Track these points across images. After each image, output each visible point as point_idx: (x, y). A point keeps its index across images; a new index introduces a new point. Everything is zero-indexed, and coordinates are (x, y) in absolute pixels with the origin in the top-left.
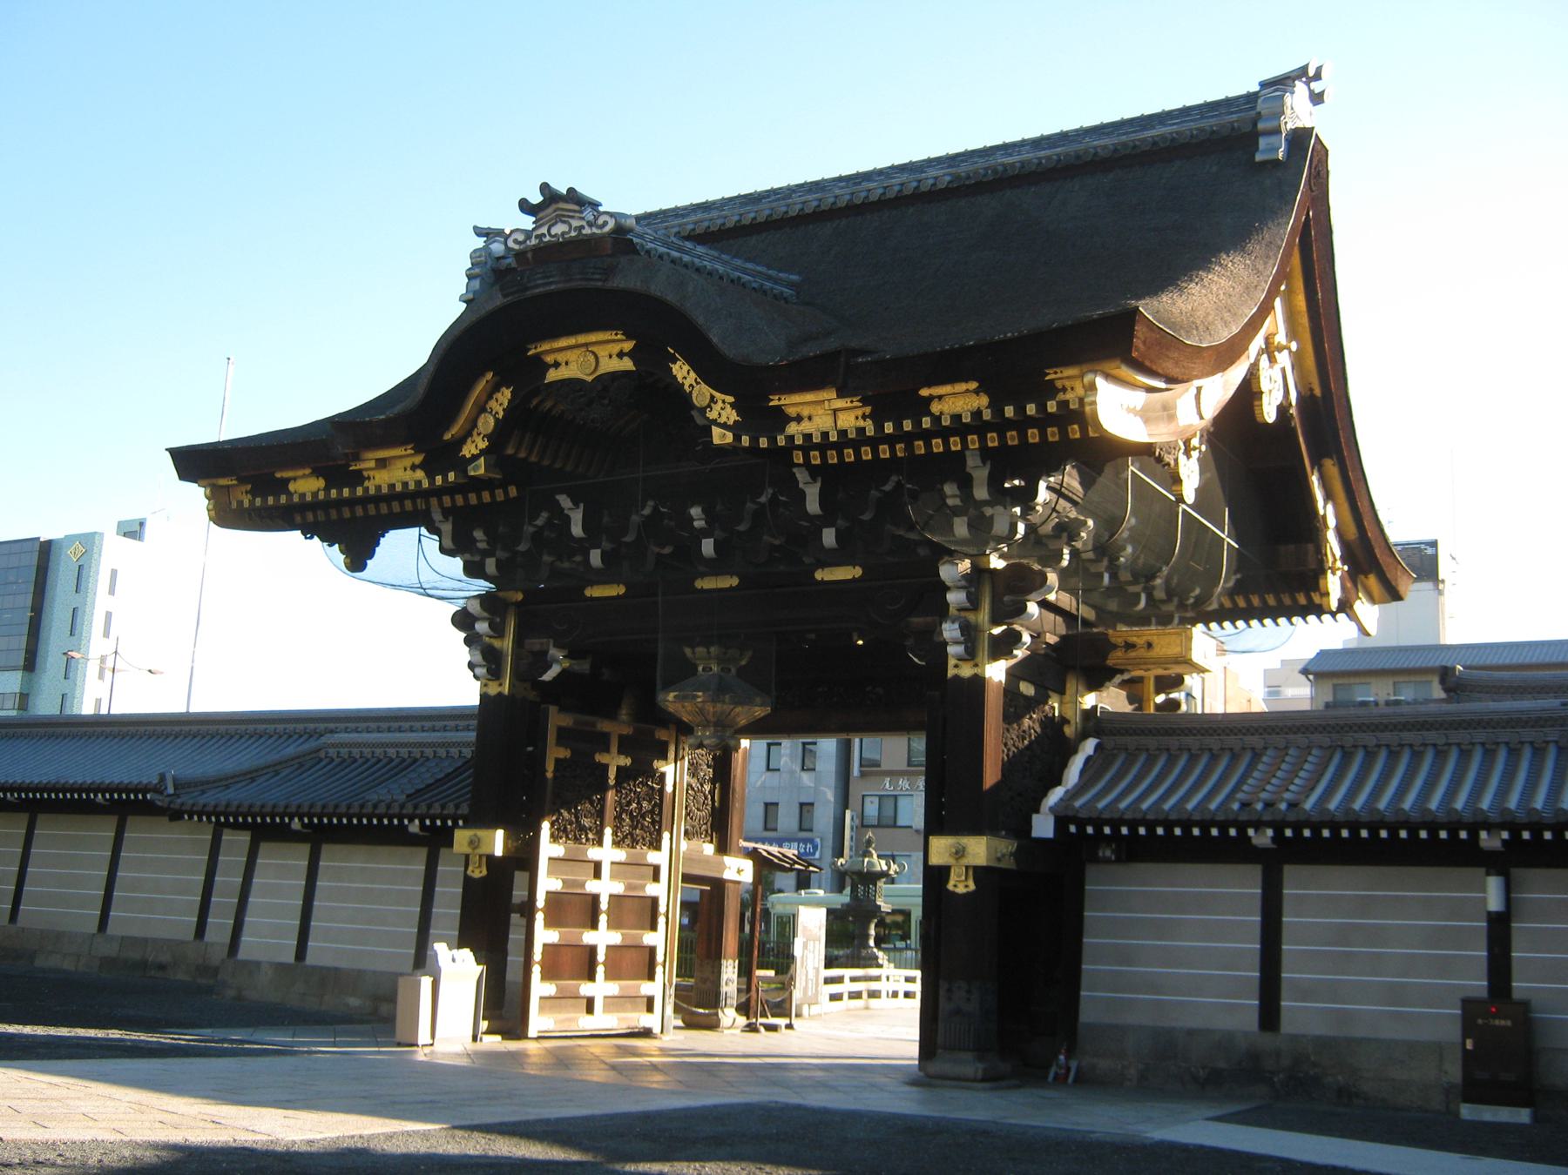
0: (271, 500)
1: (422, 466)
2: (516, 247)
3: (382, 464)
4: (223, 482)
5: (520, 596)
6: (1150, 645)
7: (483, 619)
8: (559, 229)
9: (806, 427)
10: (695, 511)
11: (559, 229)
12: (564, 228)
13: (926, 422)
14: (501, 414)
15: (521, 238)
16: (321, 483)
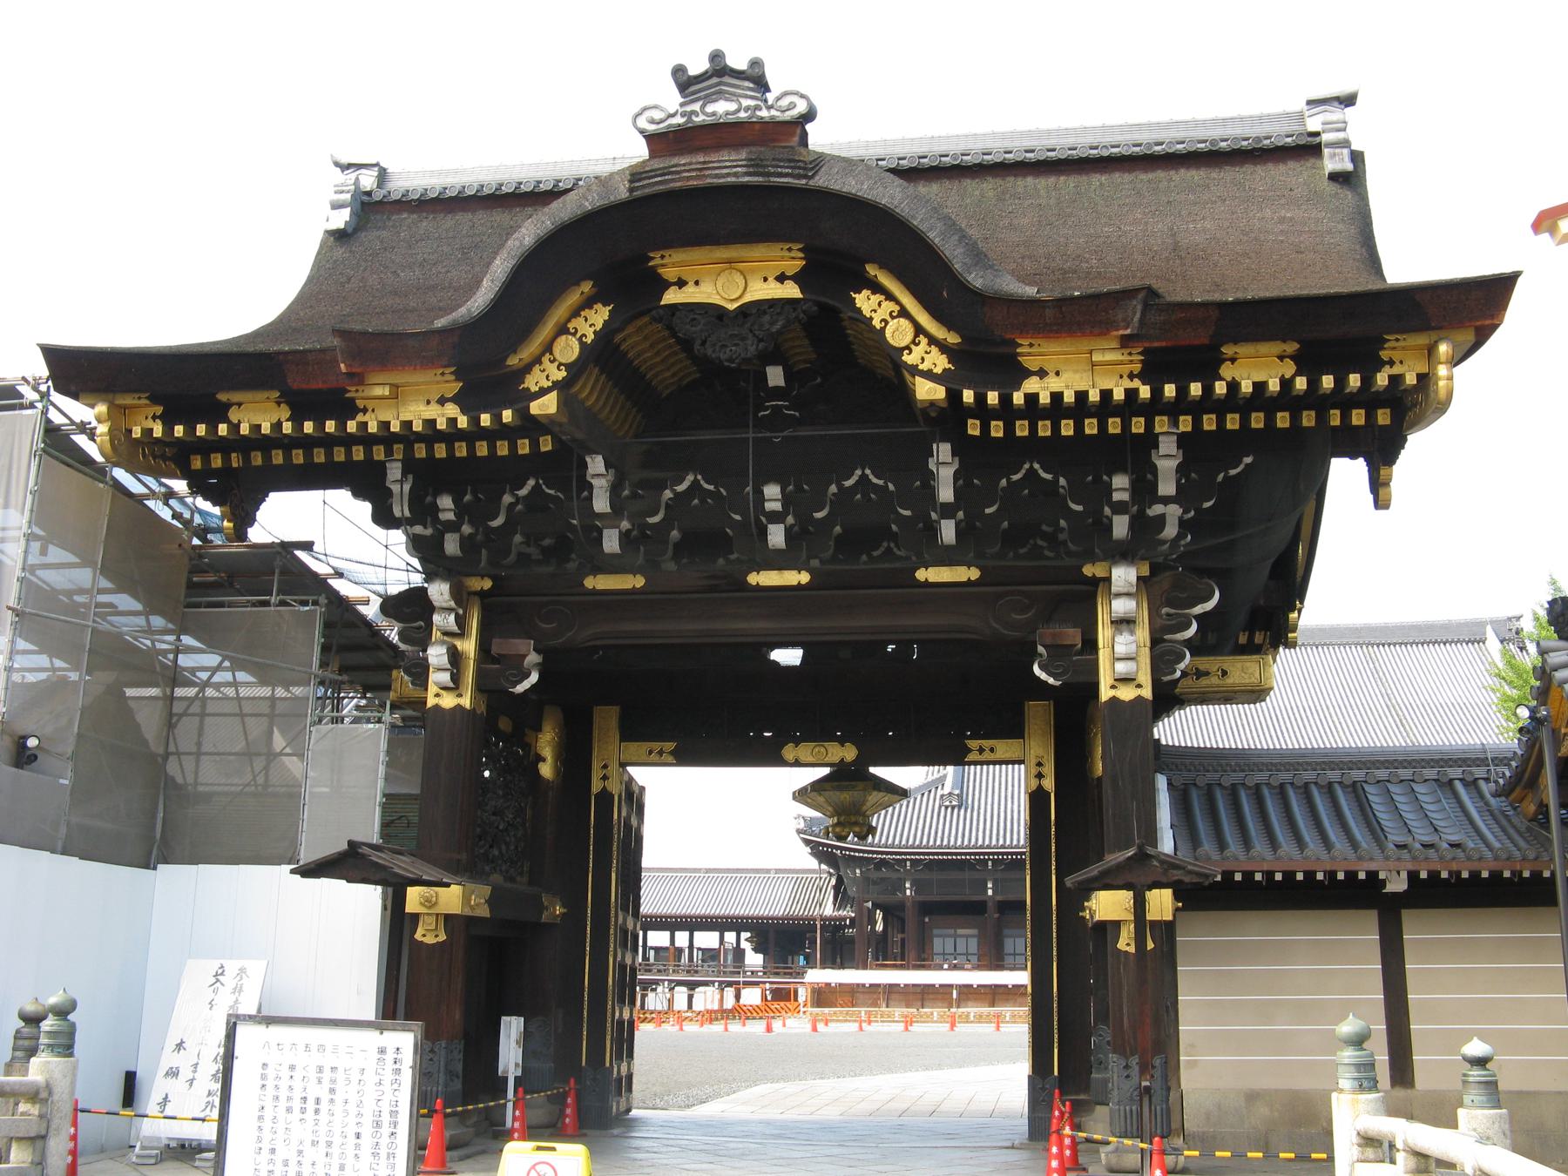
0: (201, 430)
1: (455, 400)
2: (652, 128)
3: (396, 395)
4: (127, 400)
5: (487, 584)
6: (1224, 673)
7: (450, 610)
9: (1054, 384)
10: (772, 491)
12: (732, 106)
13: (1220, 388)
14: (590, 338)
15: (658, 115)
16: (284, 412)
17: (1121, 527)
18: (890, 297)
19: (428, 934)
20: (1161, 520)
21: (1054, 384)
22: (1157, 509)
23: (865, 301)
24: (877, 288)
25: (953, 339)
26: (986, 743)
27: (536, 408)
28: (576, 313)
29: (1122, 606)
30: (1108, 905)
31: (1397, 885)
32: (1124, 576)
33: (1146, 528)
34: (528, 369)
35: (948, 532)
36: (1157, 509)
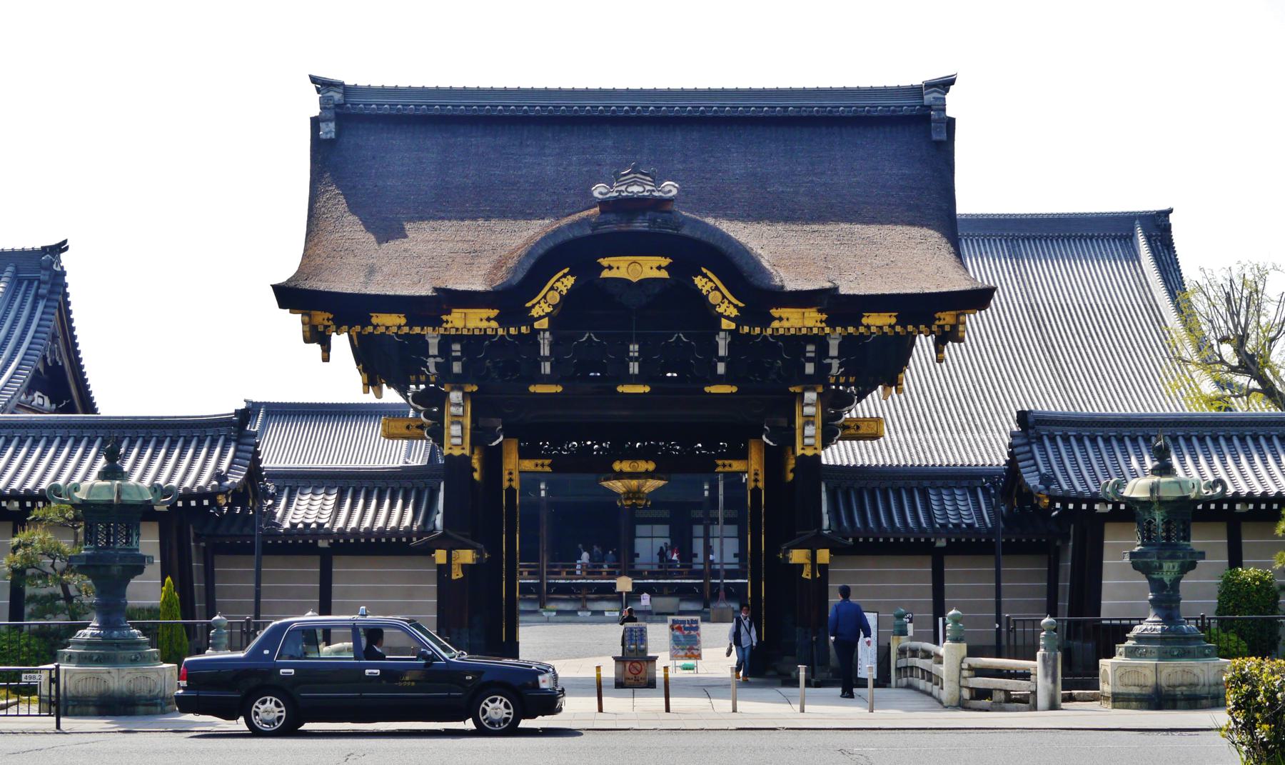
5: (475, 388)
6: (858, 428)
8: (636, 189)
11: (636, 189)
12: (641, 189)
17: (810, 369)
18: (711, 280)
19: (457, 574)
20: (830, 366)
21: (786, 324)
22: (828, 361)
23: (699, 281)
24: (705, 276)
25: (741, 305)
26: (727, 462)
27: (537, 325)
28: (558, 280)
29: (809, 410)
30: (798, 556)
31: (941, 543)
32: (810, 396)
33: (823, 370)
34: (533, 306)
35: (721, 368)
36: (828, 361)
